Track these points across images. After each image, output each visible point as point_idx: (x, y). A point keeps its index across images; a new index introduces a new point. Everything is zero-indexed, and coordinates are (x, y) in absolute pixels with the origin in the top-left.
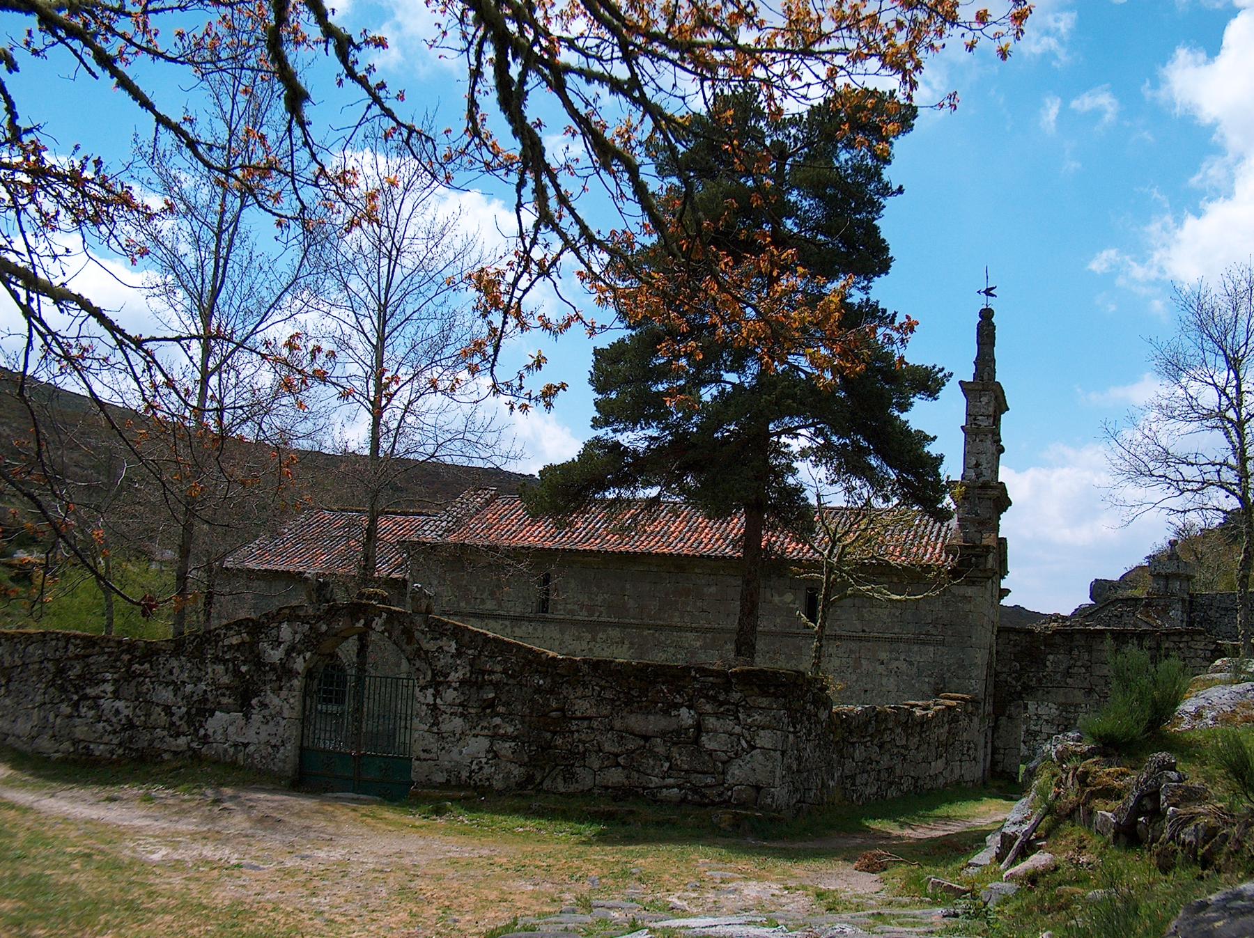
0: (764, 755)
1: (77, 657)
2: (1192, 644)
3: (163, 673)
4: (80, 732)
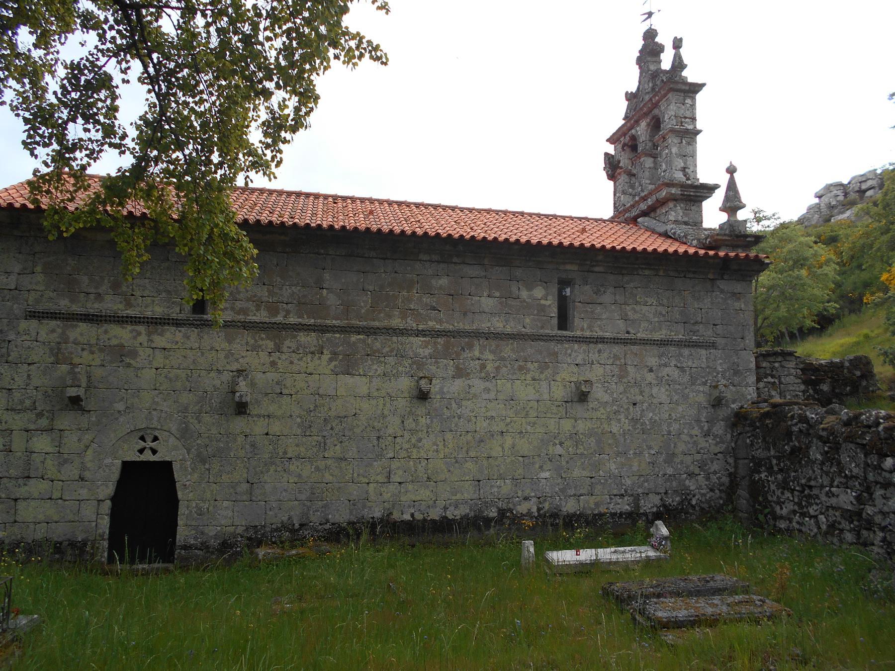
2: (784, 363)
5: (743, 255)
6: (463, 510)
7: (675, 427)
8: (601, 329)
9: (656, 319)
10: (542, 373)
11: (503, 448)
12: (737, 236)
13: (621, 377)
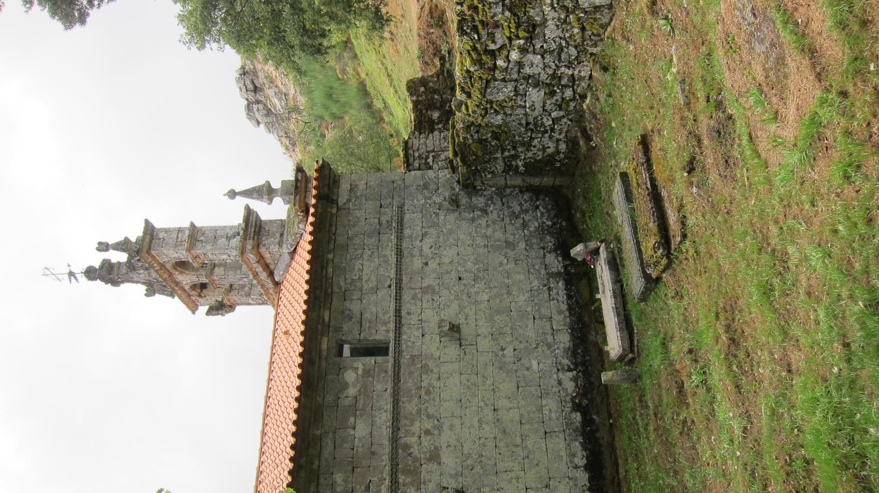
5: (315, 183)
6: (577, 446)
7: (479, 240)
8: (384, 314)
9: (376, 260)
10: (432, 371)
11: (510, 408)
12: (297, 188)
13: (434, 292)
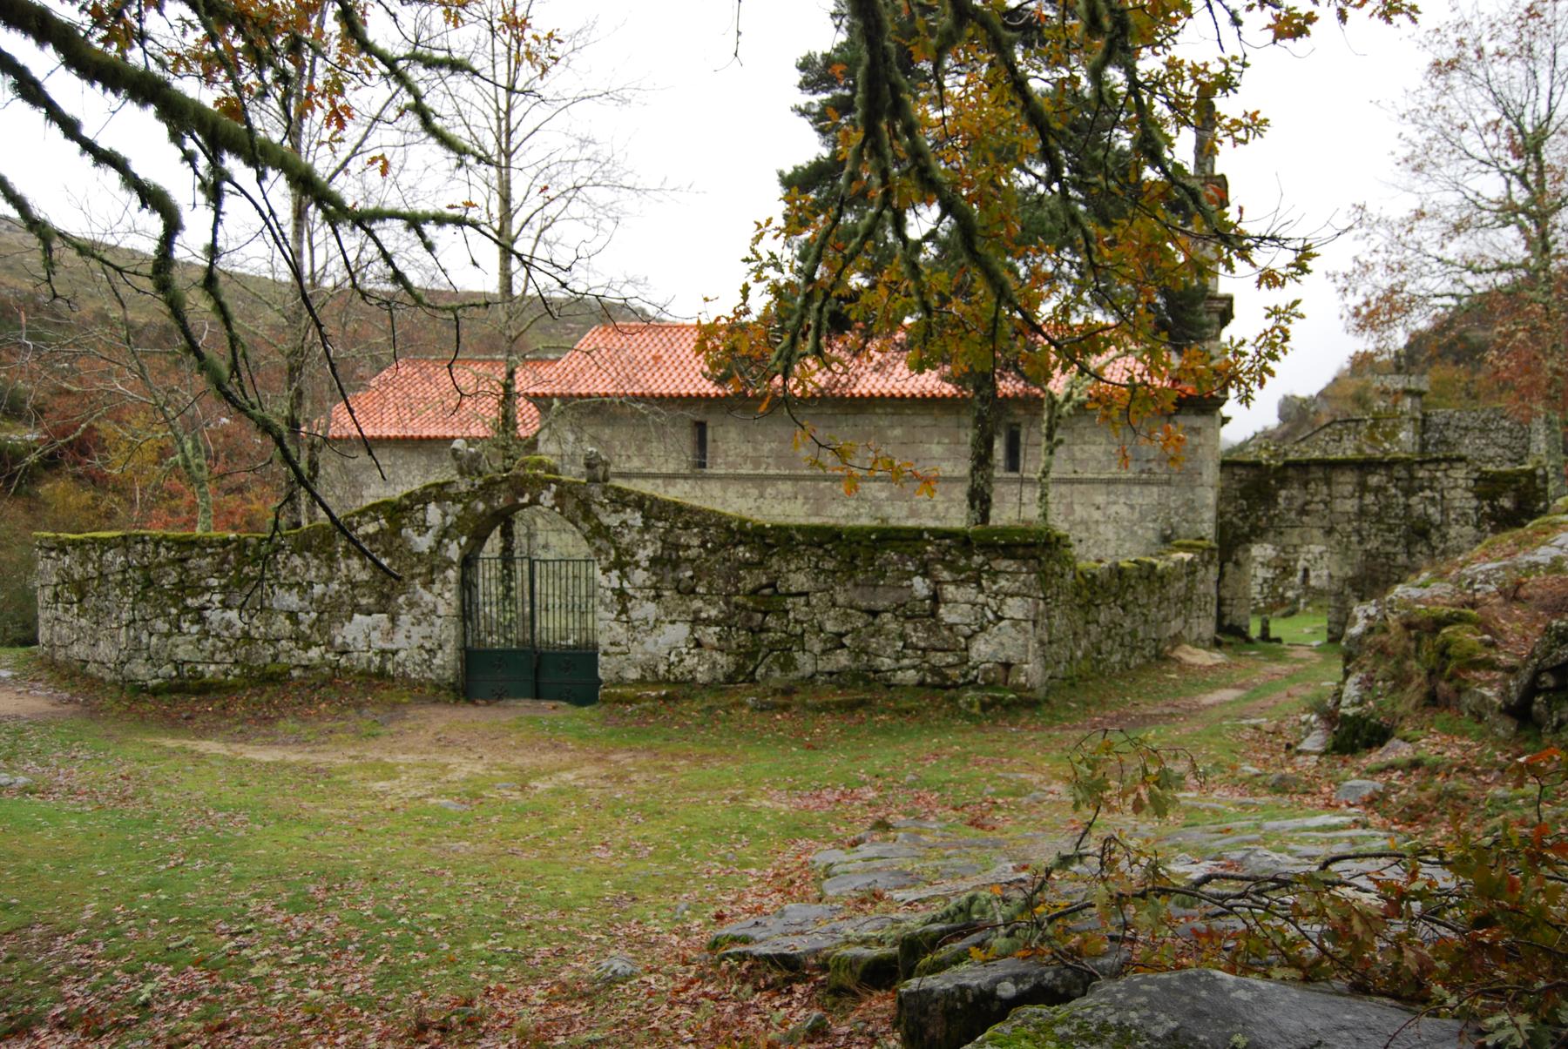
0: (1014, 626)
1: (172, 562)
3: (283, 573)
4: (181, 654)
